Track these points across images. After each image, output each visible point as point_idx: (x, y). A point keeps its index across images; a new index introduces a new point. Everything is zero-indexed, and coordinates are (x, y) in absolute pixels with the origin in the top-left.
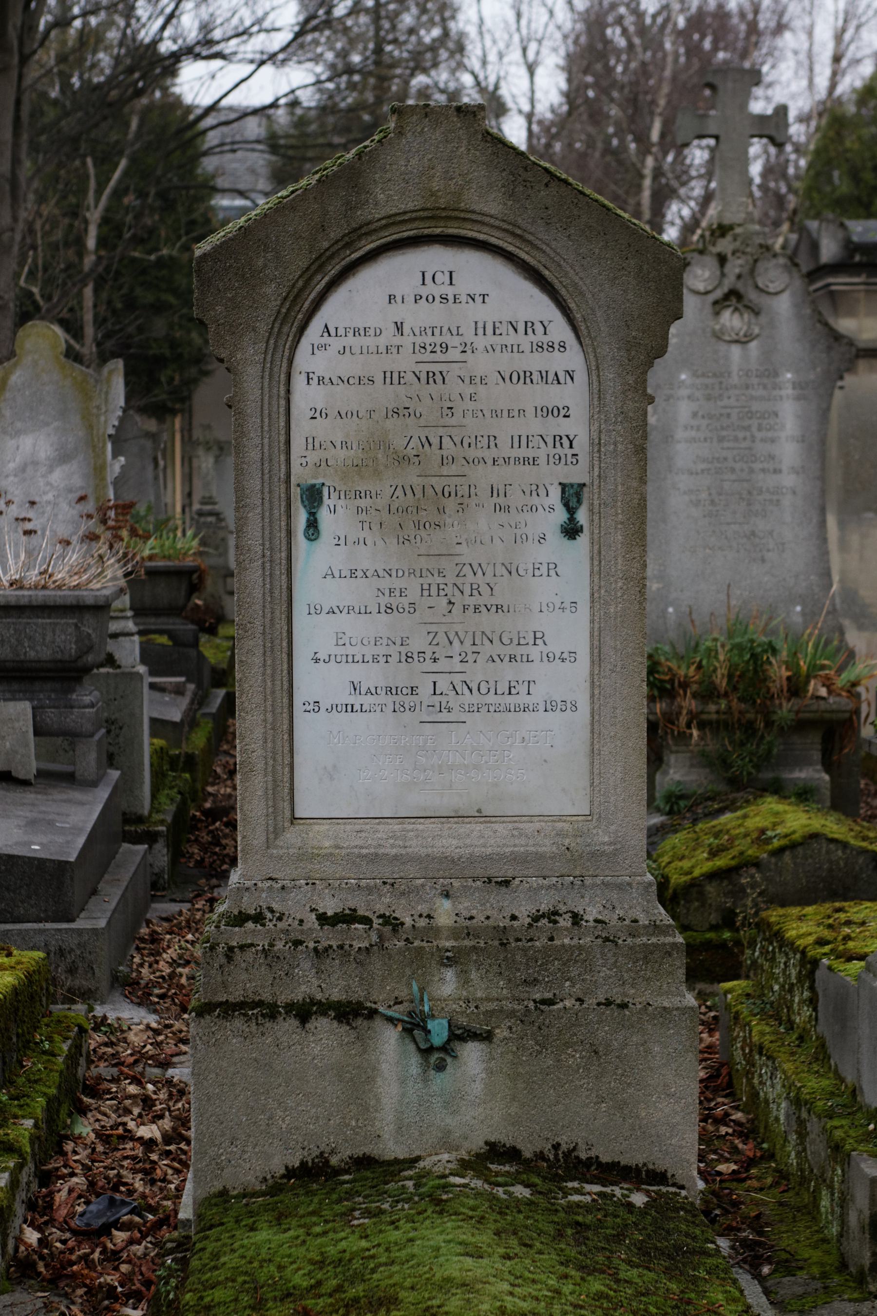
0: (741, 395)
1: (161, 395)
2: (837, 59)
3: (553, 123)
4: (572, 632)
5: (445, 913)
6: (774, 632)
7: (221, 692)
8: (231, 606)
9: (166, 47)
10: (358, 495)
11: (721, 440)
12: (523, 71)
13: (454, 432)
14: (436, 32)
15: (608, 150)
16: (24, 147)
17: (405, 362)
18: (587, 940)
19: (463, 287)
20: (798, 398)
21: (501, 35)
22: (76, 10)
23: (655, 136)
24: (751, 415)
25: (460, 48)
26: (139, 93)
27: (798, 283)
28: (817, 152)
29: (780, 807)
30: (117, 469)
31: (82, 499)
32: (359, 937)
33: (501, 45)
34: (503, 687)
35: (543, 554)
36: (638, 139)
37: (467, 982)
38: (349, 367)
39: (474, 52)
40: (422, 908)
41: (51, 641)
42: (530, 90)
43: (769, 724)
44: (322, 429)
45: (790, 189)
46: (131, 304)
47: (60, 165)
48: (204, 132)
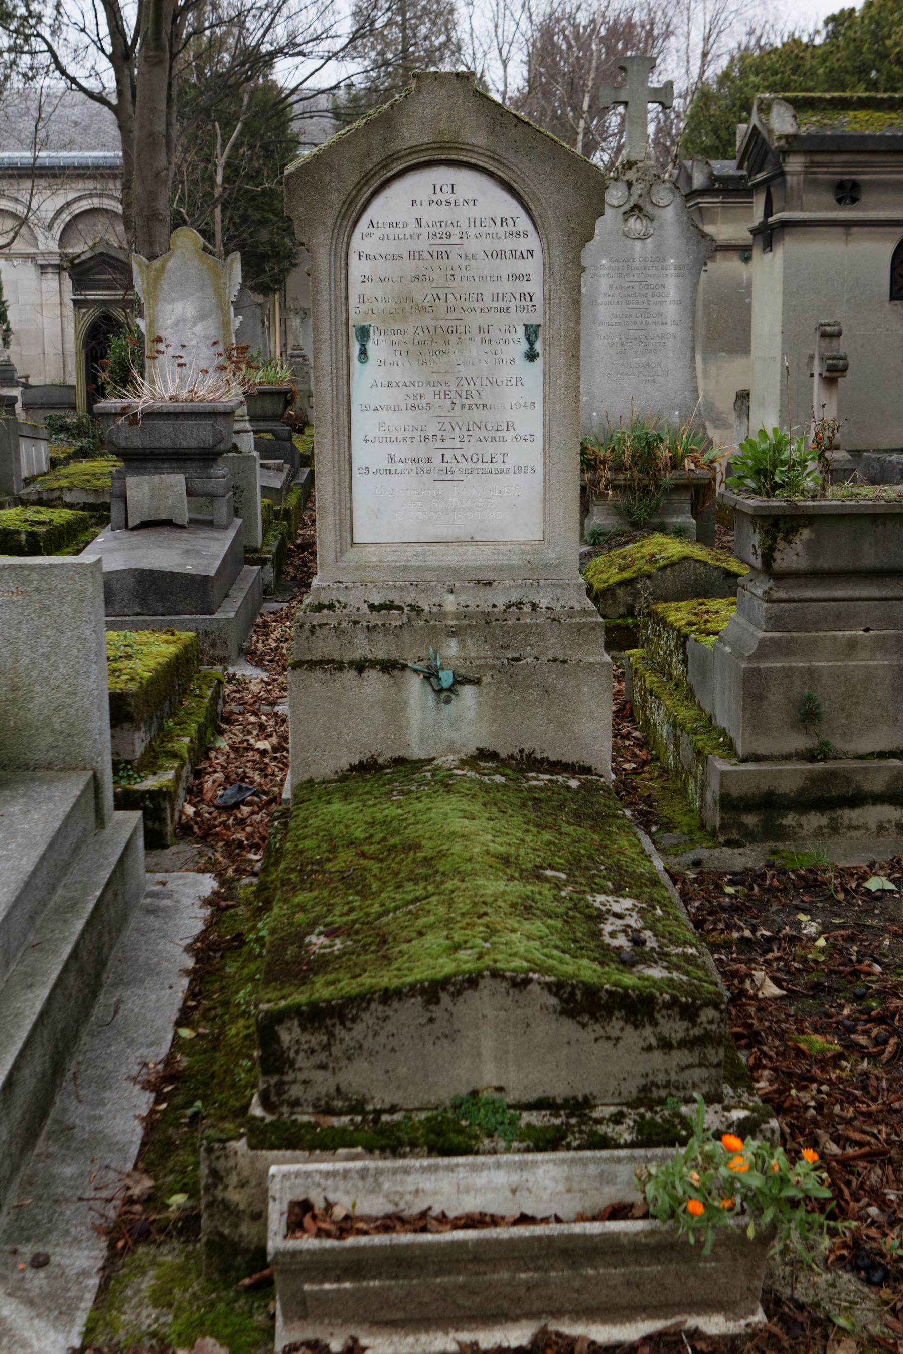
0: (641, 269)
1: (265, 278)
2: (705, 55)
3: (518, 100)
4: (532, 422)
5: (450, 603)
6: (661, 428)
7: (307, 470)
8: (313, 415)
9: (265, 48)
10: (393, 333)
11: (628, 303)
12: (499, 64)
13: (454, 291)
14: (443, 38)
15: (555, 117)
16: (174, 115)
17: (423, 245)
18: (541, 620)
19: (460, 195)
20: (678, 276)
21: (486, 41)
22: (207, 24)
23: (585, 106)
24: (647, 287)
25: (459, 49)
26: (248, 79)
27: (679, 200)
28: (692, 117)
29: (664, 540)
30: (237, 324)
31: (215, 343)
32: (395, 619)
33: (485, 47)
34: (487, 458)
35: (512, 371)
36: (574, 109)
37: (464, 647)
38: (385, 248)
39: (467, 52)
40: (436, 600)
41: (197, 436)
42: (506, 77)
43: (658, 487)
44: (369, 289)
45: (673, 141)
46: (245, 219)
47: (198, 127)
48: (292, 104)
